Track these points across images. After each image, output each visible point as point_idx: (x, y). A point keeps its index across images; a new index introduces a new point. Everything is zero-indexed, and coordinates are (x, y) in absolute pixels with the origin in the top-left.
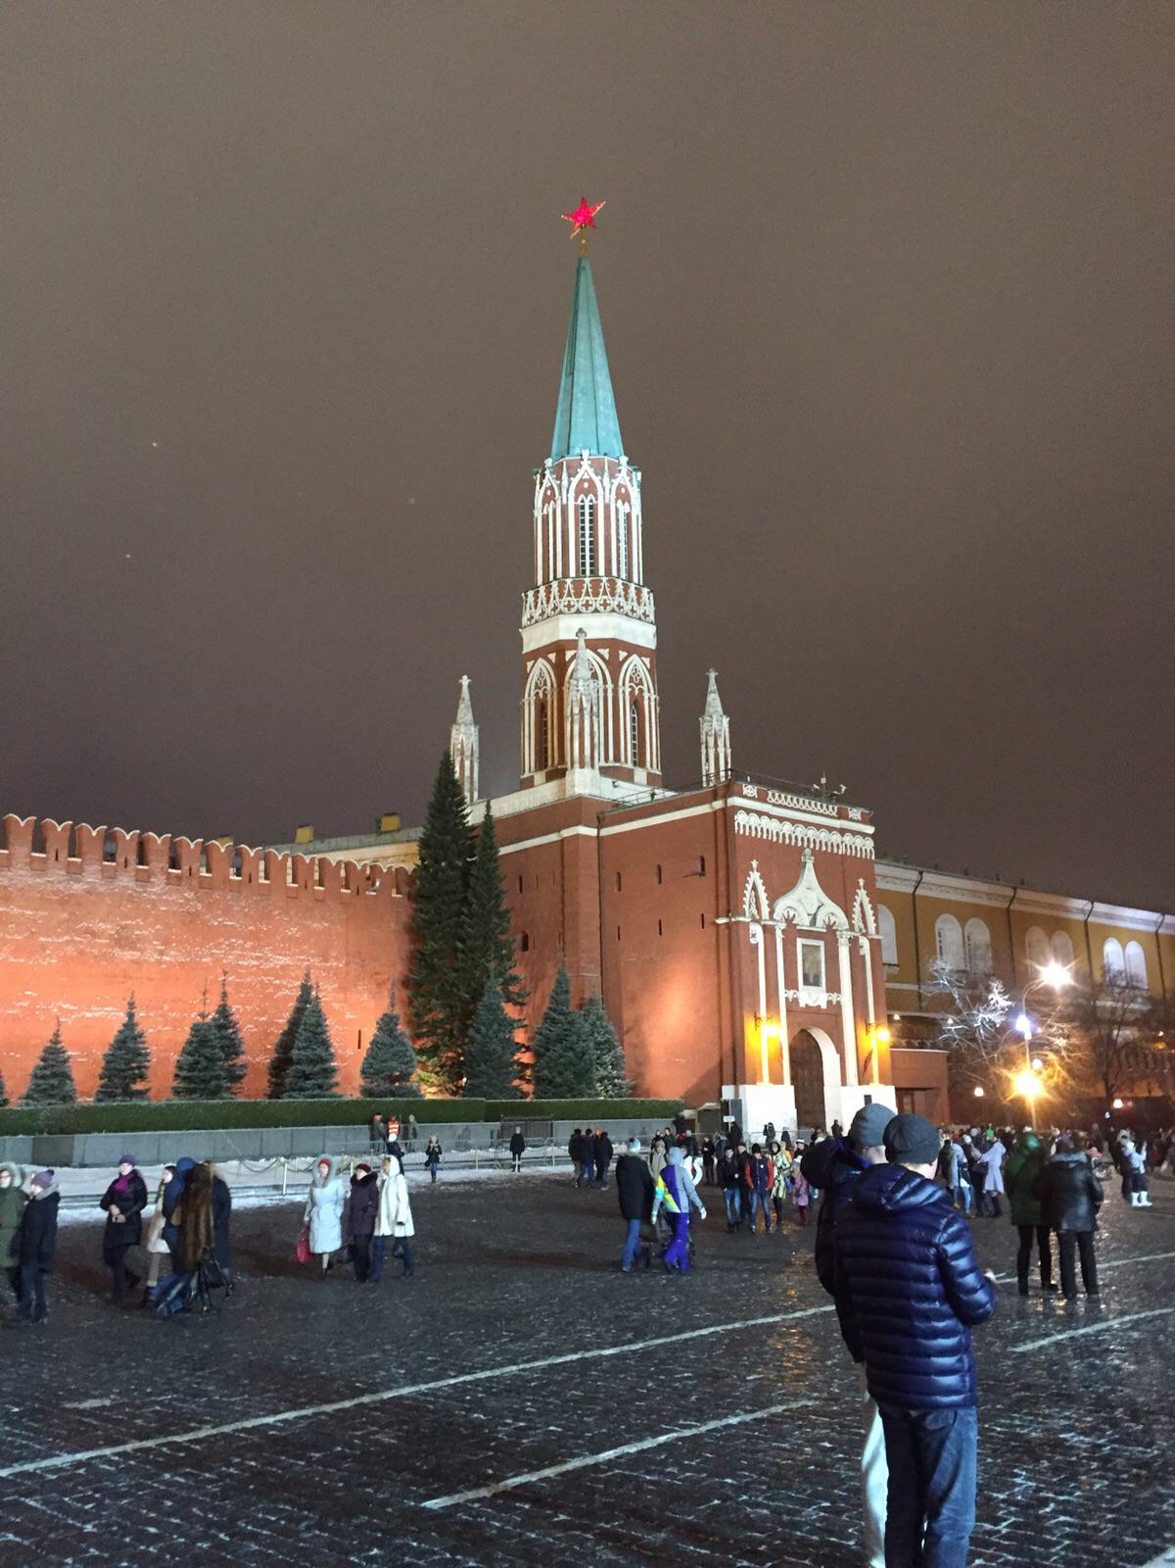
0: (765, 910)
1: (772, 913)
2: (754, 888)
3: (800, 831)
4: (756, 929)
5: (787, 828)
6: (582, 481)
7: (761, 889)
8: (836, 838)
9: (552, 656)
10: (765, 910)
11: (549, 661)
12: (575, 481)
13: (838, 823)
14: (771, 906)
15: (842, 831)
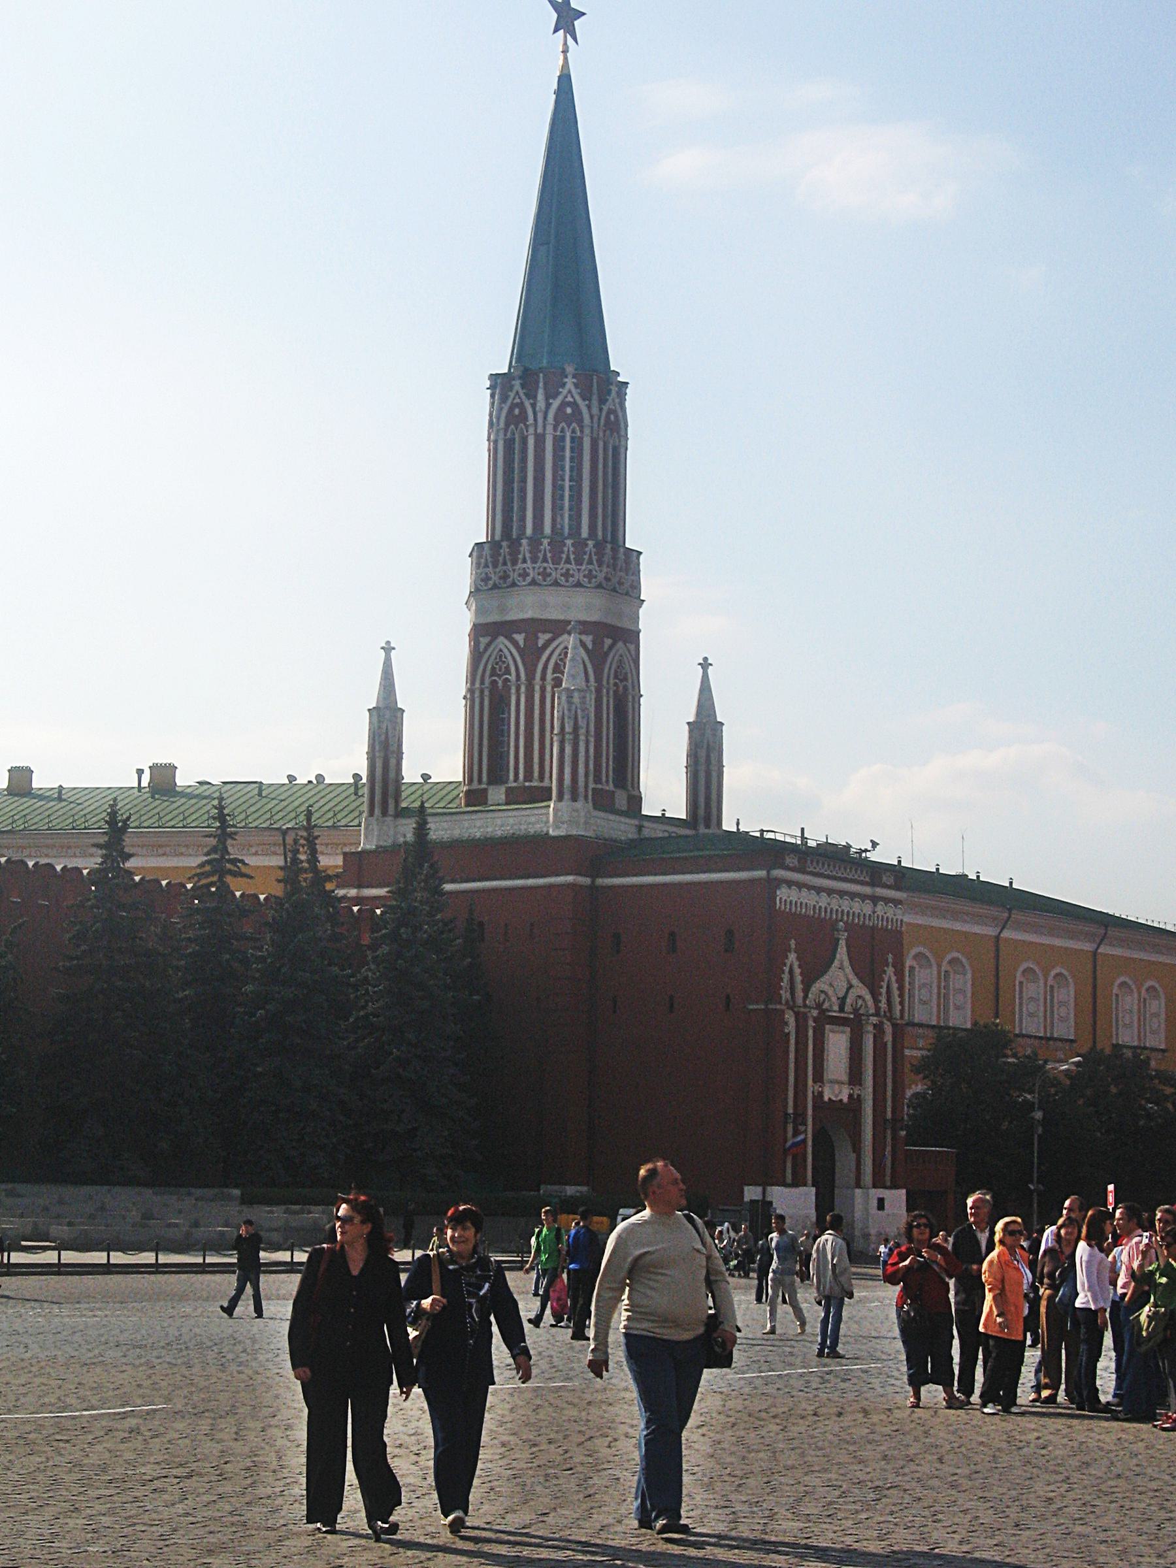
0: (800, 994)
1: (806, 997)
2: (791, 972)
3: (834, 903)
4: (790, 1017)
5: (823, 901)
6: (564, 404)
7: (797, 971)
8: (867, 908)
9: (520, 638)
10: (800, 994)
11: (515, 644)
12: (556, 404)
13: (867, 890)
14: (806, 991)
15: (875, 899)
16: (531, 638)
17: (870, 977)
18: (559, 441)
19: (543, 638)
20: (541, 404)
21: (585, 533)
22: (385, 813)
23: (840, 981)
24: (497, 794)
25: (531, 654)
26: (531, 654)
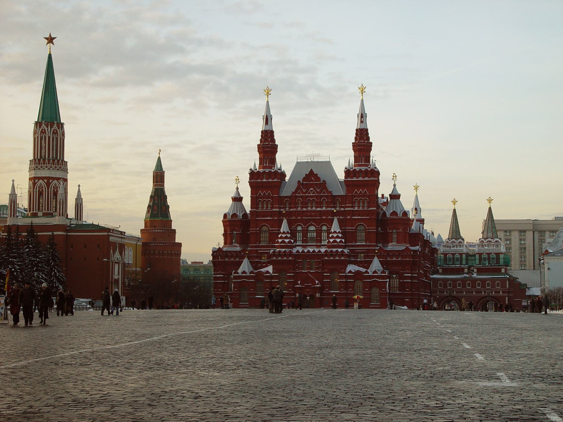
6: (54, 130)
9: (46, 181)
16: (48, 181)
17: (121, 254)
18: (53, 138)
19: (51, 181)
20: (49, 130)
21: (58, 158)
22: (14, 216)
23: (117, 255)
25: (48, 184)
26: (48, 184)
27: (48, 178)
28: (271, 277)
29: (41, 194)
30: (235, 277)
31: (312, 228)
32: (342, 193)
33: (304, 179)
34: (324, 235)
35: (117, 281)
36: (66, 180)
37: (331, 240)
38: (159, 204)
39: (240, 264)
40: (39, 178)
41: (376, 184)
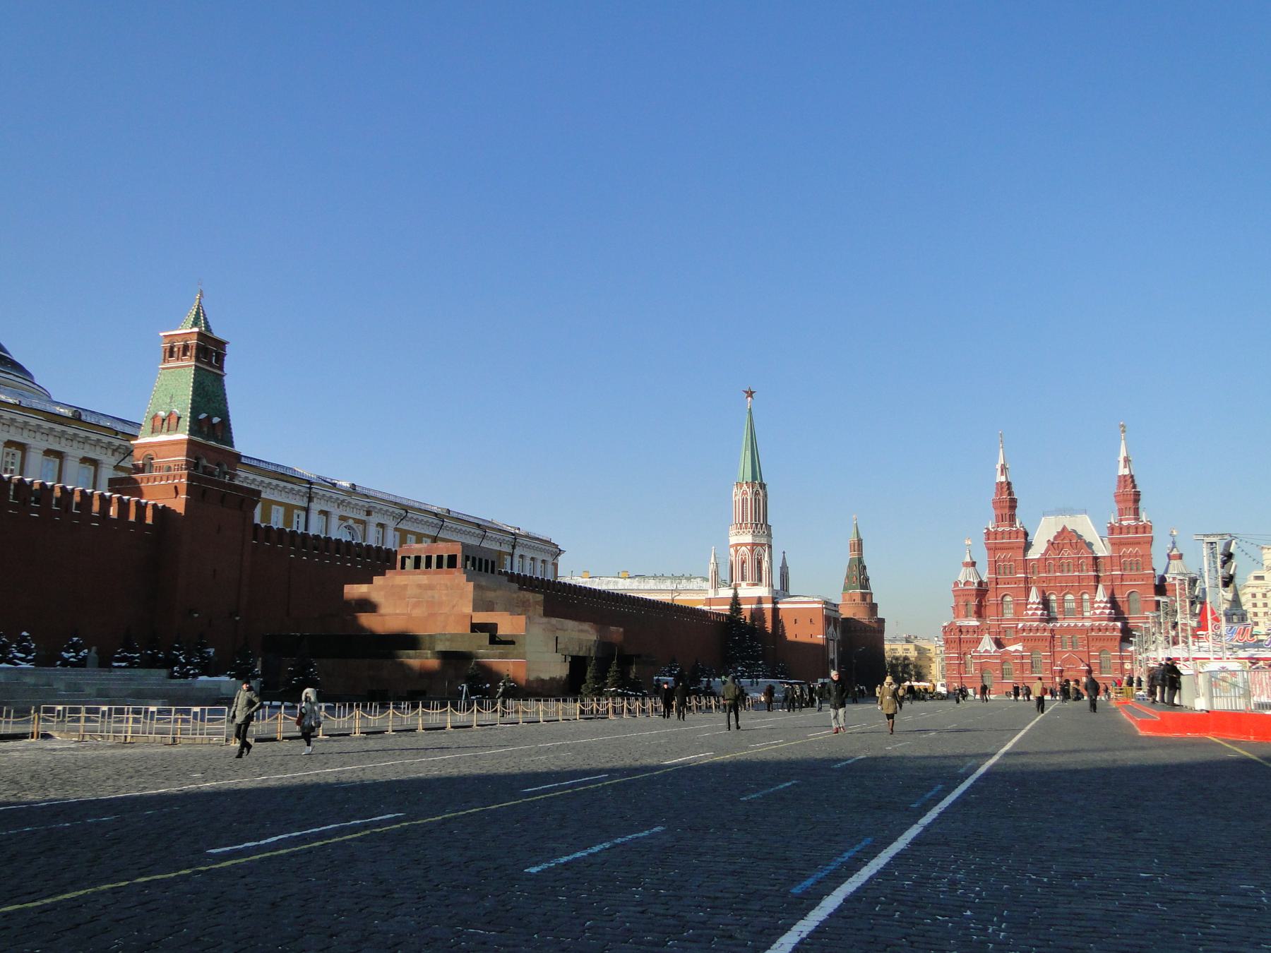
24: (744, 584)
25: (752, 551)
27: (753, 544)
28: (1022, 657)
29: (743, 563)
30: (976, 657)
31: (1069, 597)
32: (1106, 554)
33: (1055, 538)
34: (1087, 605)
35: (833, 661)
36: (770, 547)
37: (1098, 612)
38: (859, 576)
39: (978, 641)
40: (742, 545)
41: (1150, 542)
